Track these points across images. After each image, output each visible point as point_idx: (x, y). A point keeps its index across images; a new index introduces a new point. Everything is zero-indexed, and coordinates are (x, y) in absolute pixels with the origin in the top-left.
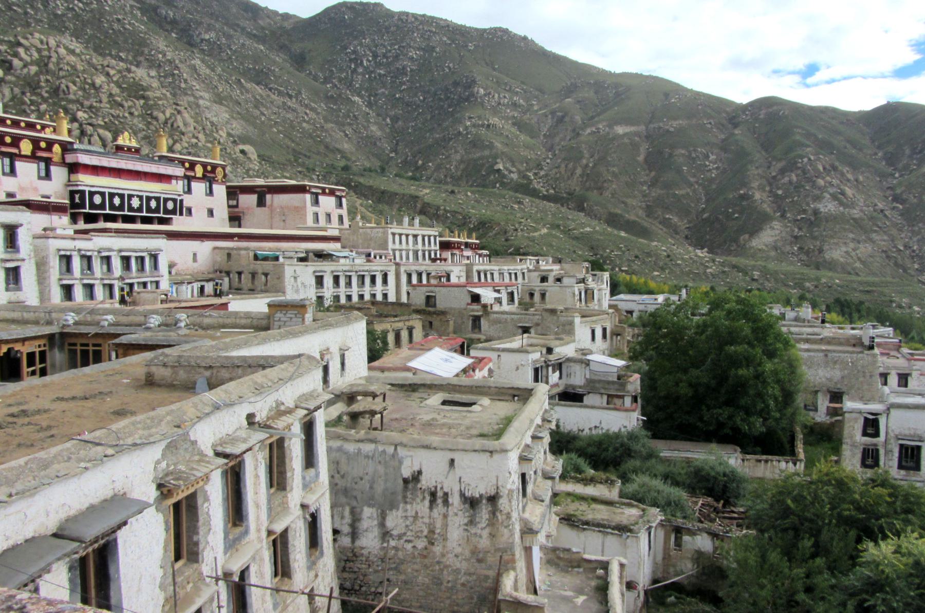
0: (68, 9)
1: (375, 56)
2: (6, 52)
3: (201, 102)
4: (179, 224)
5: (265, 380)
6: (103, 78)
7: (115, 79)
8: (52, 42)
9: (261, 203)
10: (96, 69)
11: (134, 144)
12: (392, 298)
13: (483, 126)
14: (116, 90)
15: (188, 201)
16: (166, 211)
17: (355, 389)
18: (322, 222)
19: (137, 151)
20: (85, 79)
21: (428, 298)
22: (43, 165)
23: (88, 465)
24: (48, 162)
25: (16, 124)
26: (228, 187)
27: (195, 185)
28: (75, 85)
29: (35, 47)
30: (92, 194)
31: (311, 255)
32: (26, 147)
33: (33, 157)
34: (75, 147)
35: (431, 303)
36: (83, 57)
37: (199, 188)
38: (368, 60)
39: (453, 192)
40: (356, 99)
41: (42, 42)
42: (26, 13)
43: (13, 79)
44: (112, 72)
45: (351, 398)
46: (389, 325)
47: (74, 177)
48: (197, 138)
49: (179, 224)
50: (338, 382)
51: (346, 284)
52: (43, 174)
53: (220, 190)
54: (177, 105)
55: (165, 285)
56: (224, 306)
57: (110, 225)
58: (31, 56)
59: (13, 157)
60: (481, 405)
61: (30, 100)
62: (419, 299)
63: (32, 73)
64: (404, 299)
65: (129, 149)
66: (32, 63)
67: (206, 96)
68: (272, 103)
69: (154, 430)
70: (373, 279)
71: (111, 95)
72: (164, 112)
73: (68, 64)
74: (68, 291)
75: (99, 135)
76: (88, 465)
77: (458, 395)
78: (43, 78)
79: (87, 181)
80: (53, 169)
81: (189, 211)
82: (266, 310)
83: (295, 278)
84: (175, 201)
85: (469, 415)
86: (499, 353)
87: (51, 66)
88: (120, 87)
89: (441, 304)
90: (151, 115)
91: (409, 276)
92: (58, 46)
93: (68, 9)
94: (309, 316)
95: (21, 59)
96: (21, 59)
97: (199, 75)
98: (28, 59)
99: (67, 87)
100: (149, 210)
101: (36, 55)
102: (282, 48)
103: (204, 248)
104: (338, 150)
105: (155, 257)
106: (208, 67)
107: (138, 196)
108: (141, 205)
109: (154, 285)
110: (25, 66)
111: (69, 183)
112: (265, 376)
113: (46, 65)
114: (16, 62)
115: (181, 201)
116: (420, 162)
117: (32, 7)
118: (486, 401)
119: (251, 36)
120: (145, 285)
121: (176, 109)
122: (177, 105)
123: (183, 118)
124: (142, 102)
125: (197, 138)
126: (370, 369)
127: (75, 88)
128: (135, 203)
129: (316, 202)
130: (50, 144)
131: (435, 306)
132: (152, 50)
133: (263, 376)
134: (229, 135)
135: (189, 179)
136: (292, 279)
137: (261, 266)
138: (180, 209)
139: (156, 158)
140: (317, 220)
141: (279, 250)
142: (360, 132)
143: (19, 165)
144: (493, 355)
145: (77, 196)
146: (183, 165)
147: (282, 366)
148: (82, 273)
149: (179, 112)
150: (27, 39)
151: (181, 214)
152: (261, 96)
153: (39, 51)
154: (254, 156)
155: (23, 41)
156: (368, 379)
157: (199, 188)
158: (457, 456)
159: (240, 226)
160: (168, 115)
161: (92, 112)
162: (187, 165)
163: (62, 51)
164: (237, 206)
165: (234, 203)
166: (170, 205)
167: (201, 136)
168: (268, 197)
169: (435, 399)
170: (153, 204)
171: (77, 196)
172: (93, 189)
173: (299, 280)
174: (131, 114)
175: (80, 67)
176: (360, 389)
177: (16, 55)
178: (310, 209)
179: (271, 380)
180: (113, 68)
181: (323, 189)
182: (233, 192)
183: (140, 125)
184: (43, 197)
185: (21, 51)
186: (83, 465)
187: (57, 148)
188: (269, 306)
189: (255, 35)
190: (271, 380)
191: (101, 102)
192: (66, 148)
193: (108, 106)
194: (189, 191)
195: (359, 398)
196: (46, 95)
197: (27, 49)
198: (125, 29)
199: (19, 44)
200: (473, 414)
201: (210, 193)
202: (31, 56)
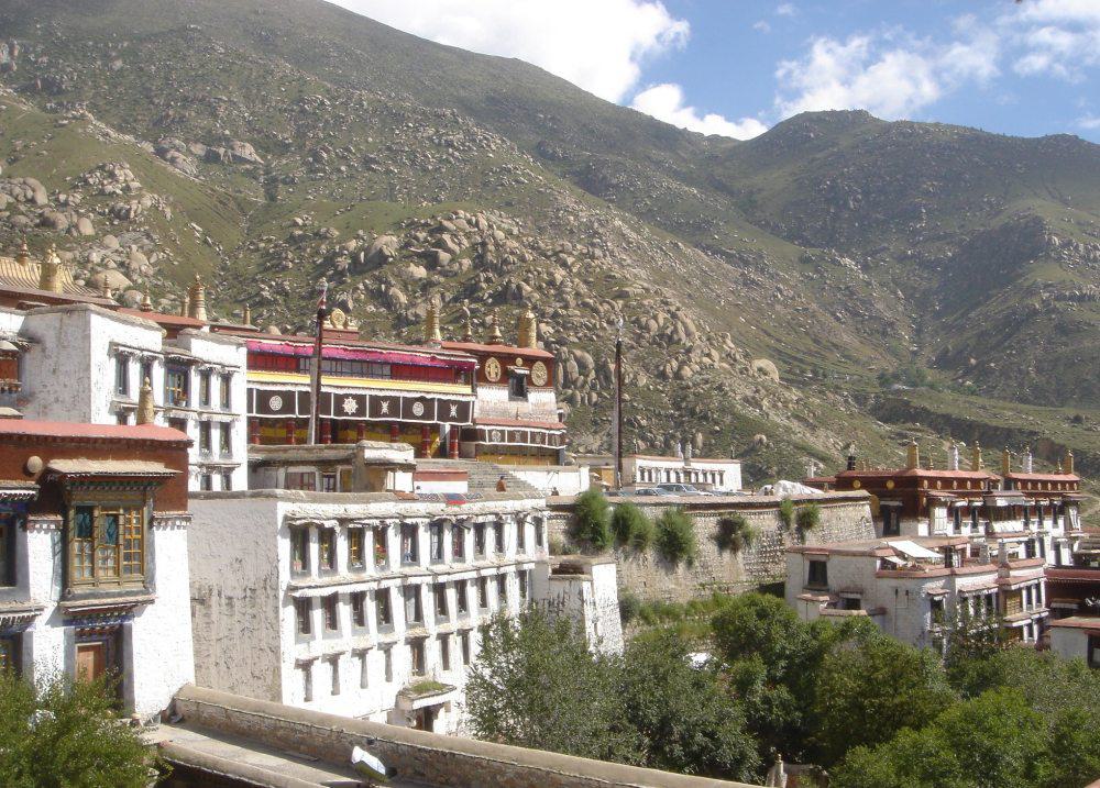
0: (441, 161)
1: (866, 193)
2: (426, 241)
6: (564, 273)
8: (483, 223)
10: (548, 257)
13: (1072, 298)
14: (583, 289)
20: (539, 273)
28: (527, 281)
29: (463, 230)
36: (525, 239)
38: (855, 200)
39: (1077, 419)
40: (847, 261)
41: (469, 222)
42: (388, 172)
43: (442, 279)
44: (570, 260)
58: (460, 244)
61: (469, 309)
63: (465, 268)
66: (464, 253)
68: (725, 276)
71: (578, 294)
72: (655, 318)
73: (512, 253)
75: (576, 359)
87: (490, 257)
88: (586, 282)
90: (637, 321)
92: (490, 227)
93: (441, 161)
95: (448, 250)
96: (448, 250)
97: (629, 243)
98: (457, 248)
99: (519, 287)
101: (465, 242)
102: (720, 187)
104: (835, 345)
106: (632, 228)
110: (452, 260)
113: (481, 257)
114: (444, 256)
116: (973, 361)
117: (395, 162)
119: (676, 175)
124: (621, 302)
132: (558, 210)
142: (858, 314)
150: (450, 219)
152: (710, 267)
153: (468, 236)
155: (446, 223)
160: (661, 322)
161: (558, 324)
163: (500, 235)
175: (529, 257)
177: (441, 244)
180: (570, 254)
185: (446, 237)
189: (675, 172)
191: (566, 307)
193: (577, 312)
196: (490, 301)
197: (454, 235)
198: (517, 182)
199: (442, 229)
202: (460, 244)
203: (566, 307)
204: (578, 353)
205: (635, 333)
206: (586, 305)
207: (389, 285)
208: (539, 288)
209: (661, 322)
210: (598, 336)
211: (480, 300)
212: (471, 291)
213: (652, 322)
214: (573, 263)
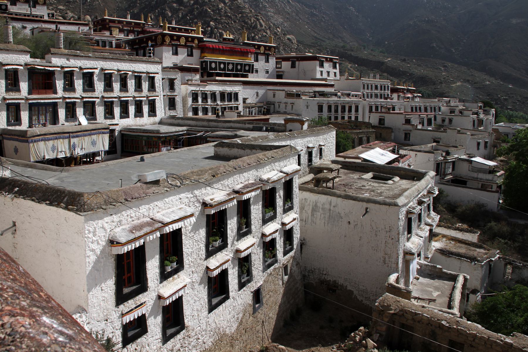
3: (269, 14)
4: (252, 78)
5: (263, 157)
6: (223, 5)
7: (228, 5)
9: (293, 66)
11: (231, 37)
12: (360, 119)
15: (256, 65)
16: (245, 71)
17: (322, 166)
18: (325, 76)
19: (232, 40)
21: (380, 120)
22: (190, 49)
23: (168, 189)
24: (192, 48)
25: (180, 30)
26: (276, 59)
27: (259, 57)
30: (211, 63)
31: (317, 94)
32: (183, 41)
33: (185, 46)
34: (205, 39)
35: (382, 122)
37: (262, 58)
45: (318, 170)
46: (352, 134)
47: (203, 55)
48: (266, 33)
49: (252, 78)
50: (317, 161)
51: (335, 110)
52: (190, 53)
53: (273, 61)
54: (257, 16)
55: (241, 108)
56: (268, 120)
57: (217, 78)
59: (177, 46)
60: (393, 181)
62: (374, 119)
64: (367, 120)
65: (229, 39)
67: (272, 10)
69: (201, 177)
70: (350, 108)
71: (226, 12)
72: (250, 20)
74: (195, 111)
75: (219, 33)
76: (168, 189)
77: (383, 173)
78: (196, 6)
79: (209, 57)
80: (194, 50)
81: (257, 71)
82: (283, 122)
83: (307, 106)
84: (249, 65)
85: (384, 185)
86: (417, 153)
88: (230, 9)
89: (387, 124)
91: (371, 108)
94: (305, 127)
99: (206, 10)
100: (237, 70)
103: (261, 91)
105: (236, 95)
107: (232, 63)
108: (233, 68)
109: (236, 108)
111: (201, 57)
112: (265, 155)
115: (253, 65)
118: (397, 179)
120: (231, 108)
121: (256, 18)
122: (257, 16)
123: (260, 22)
124: (240, 15)
125: (266, 33)
126: (336, 156)
127: (209, 10)
128: (230, 67)
129: (322, 66)
130: (193, 38)
131: (384, 124)
133: (263, 155)
134: (282, 30)
135: (257, 55)
136: (306, 107)
137: (290, 100)
138: (251, 69)
139: (241, 44)
140: (322, 75)
141: (300, 91)
143: (179, 49)
144: (412, 154)
145: (204, 64)
146: (254, 47)
147: (275, 151)
148: (202, 102)
149: (258, 20)
151: (252, 72)
154: (295, 41)
156: (334, 162)
157: (262, 58)
158: (370, 206)
159: (282, 79)
160: (252, 21)
162: (256, 47)
164: (281, 68)
165: (280, 66)
166: (247, 68)
167: (268, 32)
168: (297, 63)
169: (370, 175)
170: (239, 67)
171: (204, 64)
172: (211, 60)
173: (309, 108)
174: (235, 22)
176: (324, 166)
178: (318, 69)
179: (267, 157)
181: (326, 58)
182: (280, 60)
183: (239, 27)
184: (189, 64)
186: (165, 189)
187: (196, 42)
188: (285, 120)
190: (267, 157)
192: (200, 40)
194: (257, 60)
195: (325, 171)
200: (387, 185)
201: (267, 61)
203: (220, 17)
204: (220, 31)
205: (242, 25)
206: (227, 16)
207: (165, 10)
208: (213, 11)
209: (252, 21)
210: (229, 26)
211: (194, 14)
212: (191, 12)
213: (249, 22)
214: (228, 3)
